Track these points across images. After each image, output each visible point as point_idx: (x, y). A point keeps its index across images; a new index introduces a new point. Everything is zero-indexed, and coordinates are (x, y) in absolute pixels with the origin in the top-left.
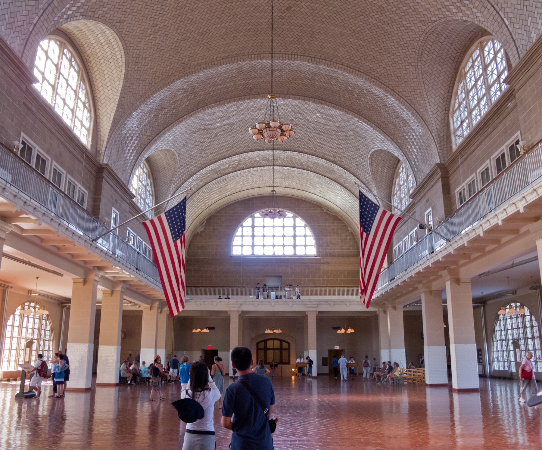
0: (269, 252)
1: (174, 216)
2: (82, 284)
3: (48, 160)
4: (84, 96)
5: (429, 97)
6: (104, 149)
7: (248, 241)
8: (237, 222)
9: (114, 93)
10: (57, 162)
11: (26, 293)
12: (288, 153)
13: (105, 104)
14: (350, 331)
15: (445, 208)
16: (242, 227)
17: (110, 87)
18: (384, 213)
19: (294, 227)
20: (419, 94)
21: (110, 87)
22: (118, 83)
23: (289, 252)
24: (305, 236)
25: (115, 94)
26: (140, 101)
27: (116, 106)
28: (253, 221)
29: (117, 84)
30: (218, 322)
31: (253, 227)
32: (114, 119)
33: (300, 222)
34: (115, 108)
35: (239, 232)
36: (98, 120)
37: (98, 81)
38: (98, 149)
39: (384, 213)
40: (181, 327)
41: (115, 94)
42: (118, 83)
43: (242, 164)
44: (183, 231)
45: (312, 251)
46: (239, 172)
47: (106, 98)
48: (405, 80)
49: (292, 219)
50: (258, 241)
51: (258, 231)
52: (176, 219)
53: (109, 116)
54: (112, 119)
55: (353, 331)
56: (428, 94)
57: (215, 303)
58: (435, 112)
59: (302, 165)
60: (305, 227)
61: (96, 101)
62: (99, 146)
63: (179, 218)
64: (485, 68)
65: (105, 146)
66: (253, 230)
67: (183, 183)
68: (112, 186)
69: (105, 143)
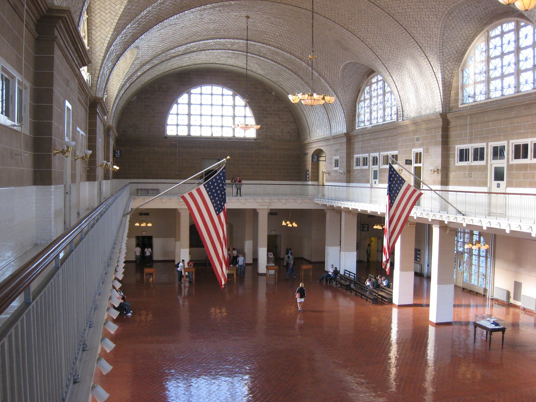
0: (206, 133)
1: (215, 188)
5: (444, 47)
7: (184, 120)
8: (173, 100)
9: (112, 16)
13: (99, 28)
15: (442, 158)
17: (109, 10)
18: (415, 191)
19: (234, 106)
20: (434, 42)
21: (109, 10)
23: (227, 133)
24: (245, 117)
25: (113, 17)
27: (112, 30)
28: (189, 99)
29: (117, 7)
31: (189, 104)
33: (240, 101)
34: (111, 33)
35: (174, 109)
39: (415, 191)
41: (113, 17)
44: (224, 203)
47: (102, 21)
48: (423, 26)
49: (231, 97)
50: (195, 120)
51: (195, 109)
52: (216, 191)
56: (444, 44)
57: (164, 200)
58: (446, 61)
59: (259, 52)
60: (245, 106)
64: (518, 49)
66: (189, 109)
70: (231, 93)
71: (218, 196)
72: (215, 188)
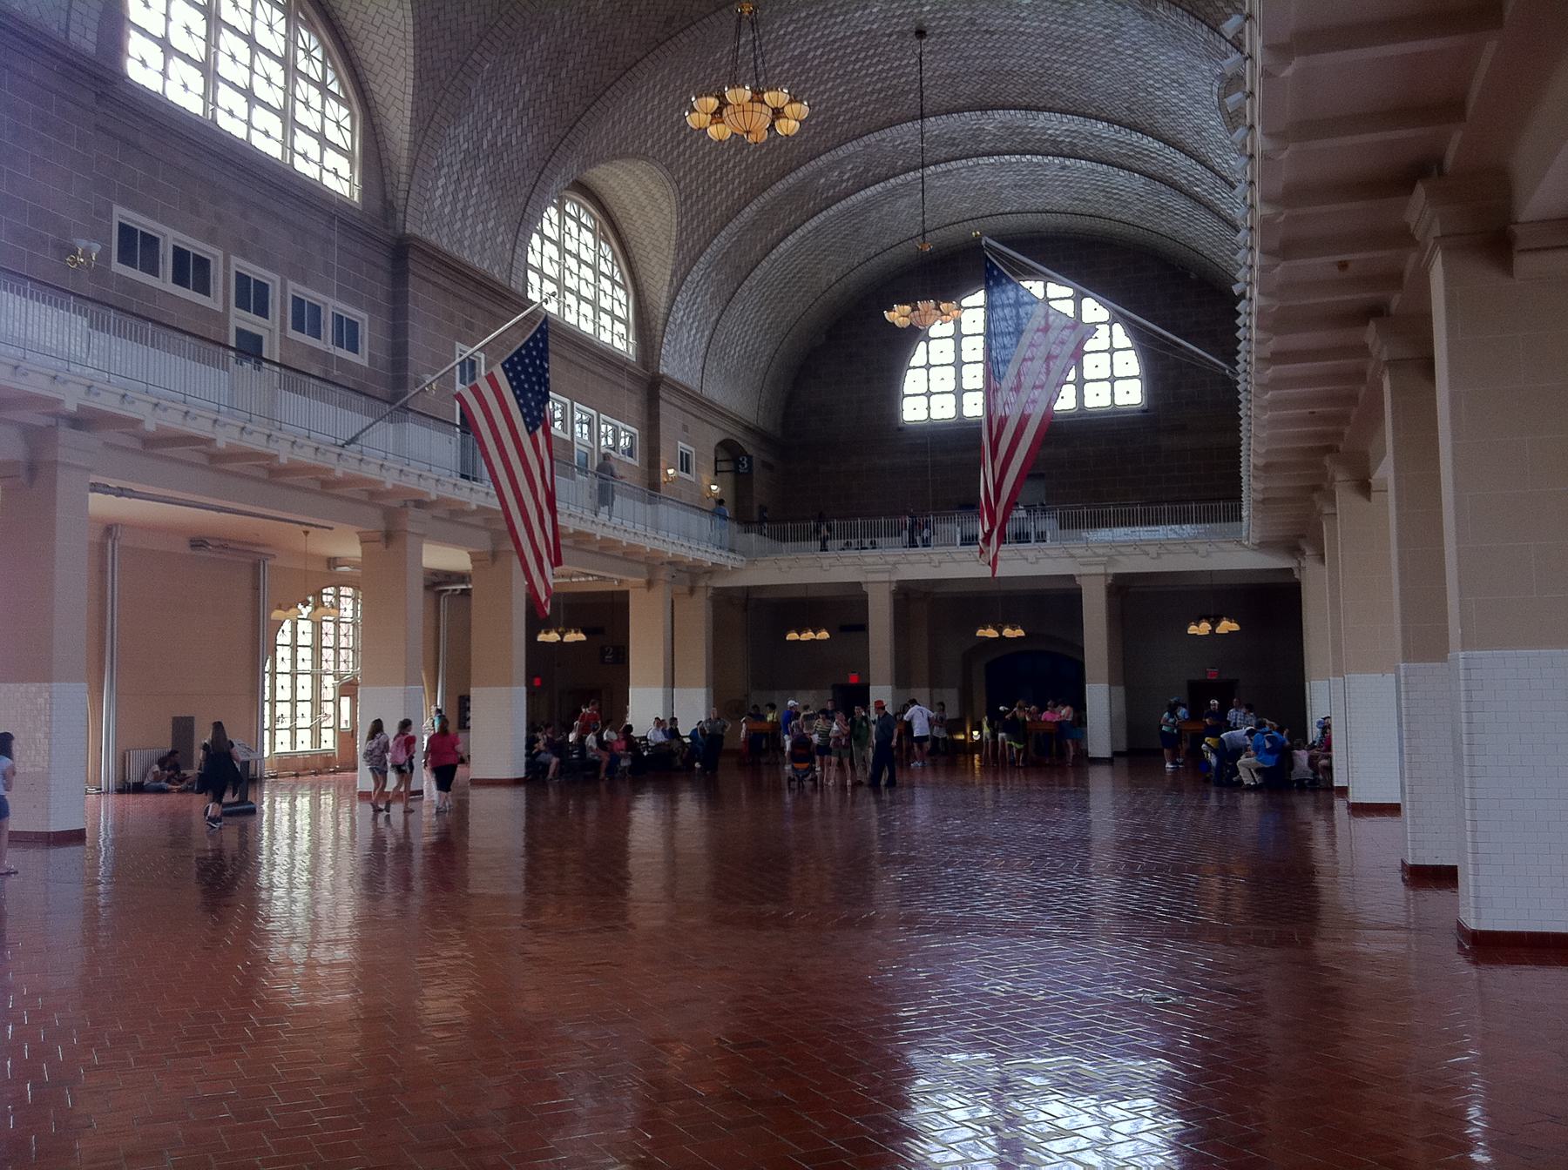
1: (525, 371)
2: (381, 546)
3: (215, 257)
4: (319, 66)
6: (402, 195)
7: (944, 379)
10: (244, 256)
11: (322, 567)
12: (999, 115)
14: (1226, 626)
16: (928, 339)
17: (384, 27)
21: (384, 27)
22: (400, 12)
25: (402, 44)
26: (480, 49)
30: (843, 610)
32: (415, 110)
34: (410, 83)
36: (376, 120)
37: (350, 18)
38: (389, 197)
40: (754, 633)
42: (400, 12)
43: (883, 165)
45: (1131, 394)
46: (879, 187)
53: (400, 105)
54: (408, 113)
55: (1235, 627)
61: (359, 70)
62: (389, 188)
63: (534, 374)
65: (403, 186)
67: (708, 243)
68: (445, 290)
69: (403, 178)
70: (1069, 292)
71: (531, 389)
72: (525, 367)
